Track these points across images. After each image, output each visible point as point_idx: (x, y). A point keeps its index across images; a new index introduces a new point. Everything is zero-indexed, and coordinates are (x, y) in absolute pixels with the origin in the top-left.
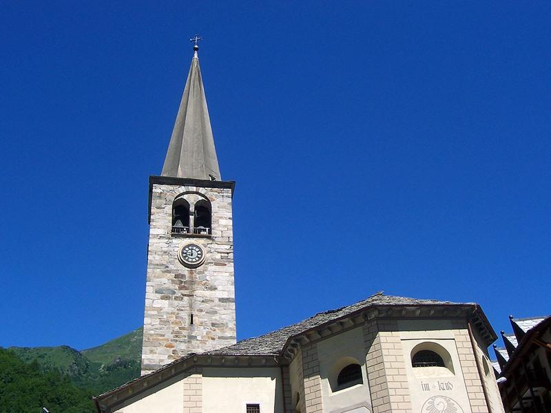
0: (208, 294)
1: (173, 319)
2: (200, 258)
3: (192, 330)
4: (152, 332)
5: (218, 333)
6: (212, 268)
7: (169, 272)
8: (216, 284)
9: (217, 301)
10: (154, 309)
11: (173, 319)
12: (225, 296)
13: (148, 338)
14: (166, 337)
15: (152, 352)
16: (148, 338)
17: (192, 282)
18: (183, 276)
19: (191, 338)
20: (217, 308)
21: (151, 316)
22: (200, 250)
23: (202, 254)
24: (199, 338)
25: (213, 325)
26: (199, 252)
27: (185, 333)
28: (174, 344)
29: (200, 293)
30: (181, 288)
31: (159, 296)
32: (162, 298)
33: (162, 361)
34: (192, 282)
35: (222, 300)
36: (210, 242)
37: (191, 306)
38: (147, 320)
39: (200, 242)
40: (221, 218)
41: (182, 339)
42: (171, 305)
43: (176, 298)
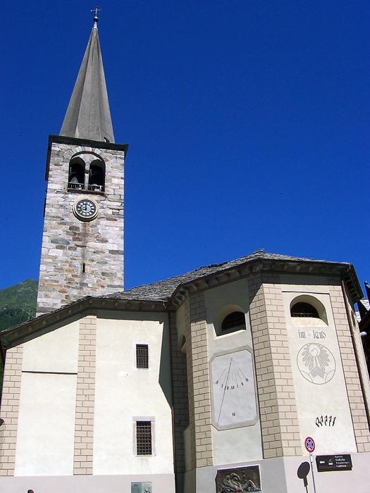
0: (99, 245)
1: (67, 267)
2: (93, 213)
3: (84, 278)
4: (47, 278)
5: (107, 281)
6: (103, 222)
7: (65, 224)
8: (107, 237)
9: (107, 253)
10: (50, 257)
11: (67, 267)
12: (115, 248)
13: (44, 284)
15: (46, 296)
16: (44, 284)
17: (85, 234)
18: (77, 228)
19: (83, 285)
20: (107, 259)
21: (47, 264)
22: (94, 205)
23: (95, 209)
24: (90, 285)
25: (103, 274)
26: (93, 208)
27: (77, 280)
28: (67, 289)
29: (93, 244)
30: (74, 240)
31: (54, 245)
32: (57, 248)
33: (55, 304)
34: (85, 234)
35: (112, 252)
37: (83, 256)
38: (42, 267)
39: (94, 198)
40: (114, 177)
41: (74, 286)
42: (65, 254)
43: (70, 248)
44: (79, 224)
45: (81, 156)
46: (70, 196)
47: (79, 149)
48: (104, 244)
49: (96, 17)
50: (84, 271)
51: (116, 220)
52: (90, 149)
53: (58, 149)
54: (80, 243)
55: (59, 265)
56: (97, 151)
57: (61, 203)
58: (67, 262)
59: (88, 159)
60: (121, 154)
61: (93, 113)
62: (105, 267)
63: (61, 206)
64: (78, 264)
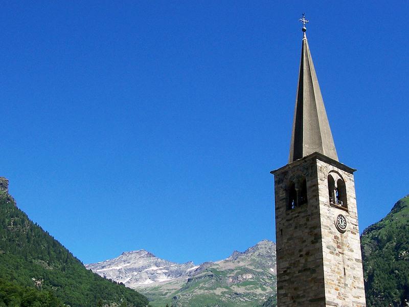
0: (350, 253)
1: (336, 270)
6: (350, 234)
7: (331, 233)
9: (354, 260)
12: (358, 258)
14: (335, 283)
18: (338, 238)
19: (346, 285)
24: (349, 286)
30: (338, 247)
31: (329, 250)
33: (334, 299)
36: (347, 214)
38: (325, 268)
42: (335, 258)
44: (338, 234)
45: (332, 174)
46: (332, 209)
47: (331, 168)
48: (352, 253)
49: (305, 28)
50: (345, 274)
51: (355, 234)
52: (336, 169)
53: (320, 166)
54: (340, 251)
55: (333, 267)
56: (340, 171)
57: (328, 215)
58: (336, 265)
59: (336, 177)
60: (352, 177)
61: (326, 131)
62: (355, 272)
63: (328, 217)
64: (341, 267)
